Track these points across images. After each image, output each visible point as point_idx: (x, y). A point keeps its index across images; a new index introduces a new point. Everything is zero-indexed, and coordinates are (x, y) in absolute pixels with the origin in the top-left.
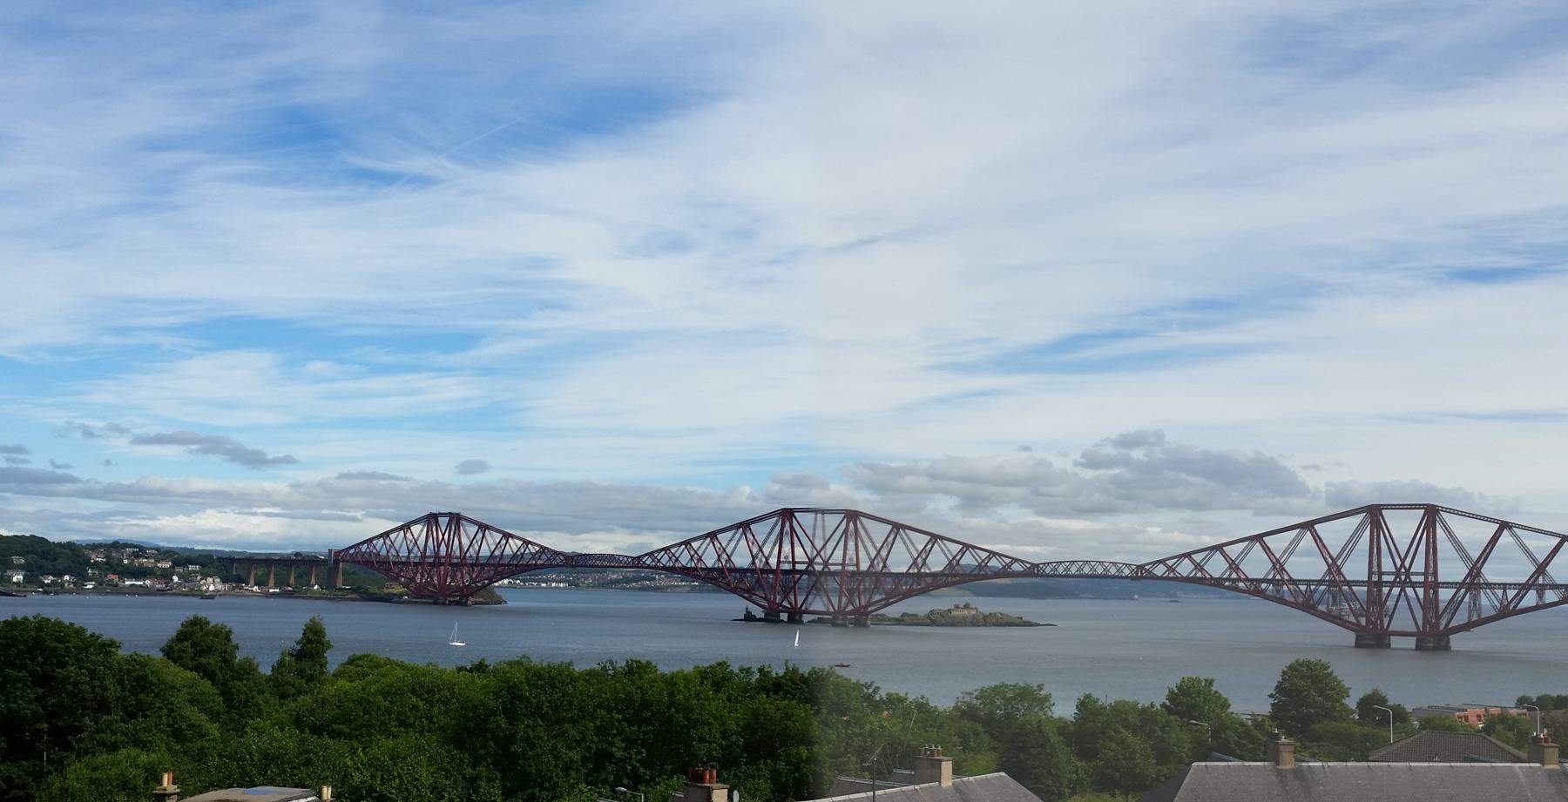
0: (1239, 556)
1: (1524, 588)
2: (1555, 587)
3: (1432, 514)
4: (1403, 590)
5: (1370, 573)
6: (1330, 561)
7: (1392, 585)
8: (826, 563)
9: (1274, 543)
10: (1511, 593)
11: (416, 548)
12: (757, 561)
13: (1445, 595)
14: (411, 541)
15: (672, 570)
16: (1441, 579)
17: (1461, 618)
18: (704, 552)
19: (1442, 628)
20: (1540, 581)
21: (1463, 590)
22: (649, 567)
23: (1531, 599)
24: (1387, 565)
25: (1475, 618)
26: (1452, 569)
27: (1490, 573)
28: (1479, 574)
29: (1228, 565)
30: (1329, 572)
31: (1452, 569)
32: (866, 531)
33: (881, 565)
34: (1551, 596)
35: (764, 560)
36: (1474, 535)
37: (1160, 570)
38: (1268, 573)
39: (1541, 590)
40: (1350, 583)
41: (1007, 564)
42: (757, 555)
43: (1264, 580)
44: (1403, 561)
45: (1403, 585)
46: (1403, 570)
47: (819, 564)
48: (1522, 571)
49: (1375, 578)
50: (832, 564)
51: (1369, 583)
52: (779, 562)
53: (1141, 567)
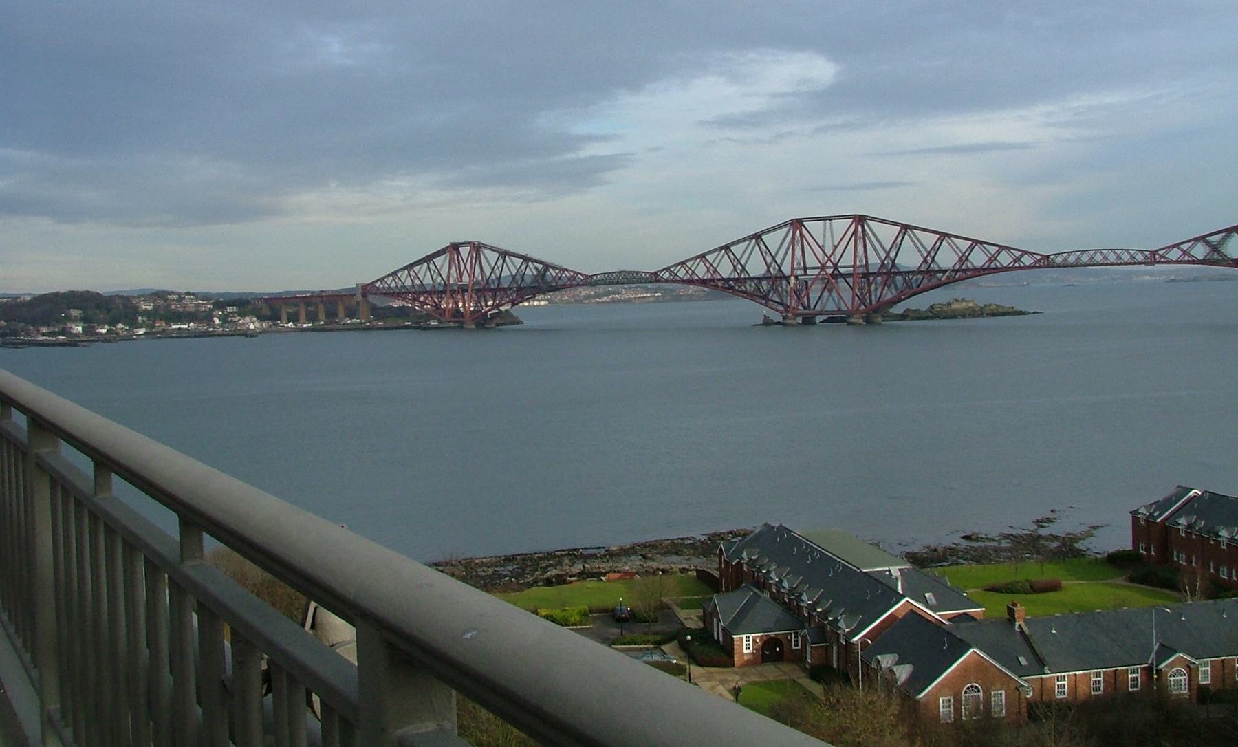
0: (714, 262)
6: (769, 259)
8: (836, 267)
11: (440, 278)
12: (771, 270)
14: (434, 271)
15: (690, 282)
18: (696, 268)
22: (667, 281)
29: (706, 269)
30: (768, 270)
32: (484, 255)
33: (496, 283)
35: (777, 267)
38: (731, 274)
41: (572, 276)
42: (771, 264)
43: (732, 280)
47: (828, 267)
50: (841, 267)
52: (793, 269)
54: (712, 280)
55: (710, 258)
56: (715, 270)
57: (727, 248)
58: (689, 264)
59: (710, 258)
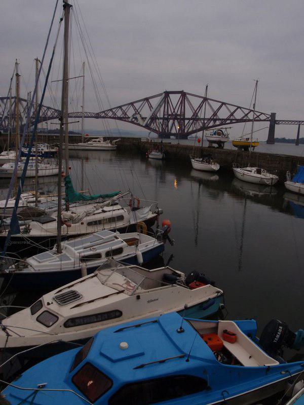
1: (210, 119)
2: (219, 119)
3: (183, 94)
4: (174, 121)
5: (164, 115)
7: (171, 119)
9: (137, 105)
10: (206, 121)
13: (186, 121)
16: (186, 117)
17: (190, 130)
19: (186, 131)
20: (215, 118)
21: (191, 121)
23: (211, 124)
24: (170, 113)
25: (195, 129)
26: (189, 114)
27: (201, 115)
28: (197, 116)
31: (189, 114)
34: (218, 123)
36: (196, 102)
37: (103, 115)
39: (215, 120)
40: (158, 119)
44: (174, 111)
45: (174, 119)
46: (174, 113)
48: (209, 114)
49: (166, 116)
51: (164, 119)
53: (98, 114)
54: (123, 118)
55: (124, 108)
56: (126, 114)
57: (132, 104)
58: (114, 110)
59: (124, 108)
